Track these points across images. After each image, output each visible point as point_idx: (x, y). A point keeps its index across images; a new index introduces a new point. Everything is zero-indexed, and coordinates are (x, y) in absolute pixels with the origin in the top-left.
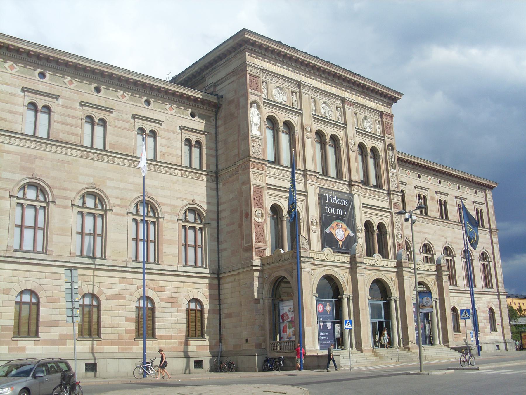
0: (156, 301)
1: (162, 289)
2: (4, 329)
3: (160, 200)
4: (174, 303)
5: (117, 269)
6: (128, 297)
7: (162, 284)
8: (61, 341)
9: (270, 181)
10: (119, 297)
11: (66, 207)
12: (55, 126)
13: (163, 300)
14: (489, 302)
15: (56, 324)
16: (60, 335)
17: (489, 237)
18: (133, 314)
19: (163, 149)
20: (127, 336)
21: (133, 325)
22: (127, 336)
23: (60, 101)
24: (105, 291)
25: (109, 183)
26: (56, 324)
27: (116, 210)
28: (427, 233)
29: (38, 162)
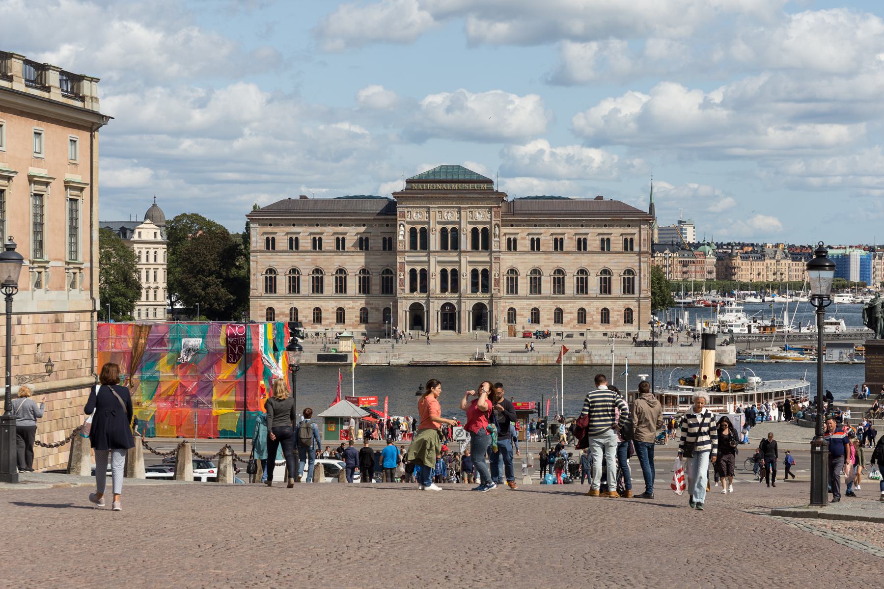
0: (369, 309)
1: (372, 304)
2: (309, 321)
3: (371, 267)
4: (377, 310)
5: (351, 298)
6: (356, 308)
7: (371, 302)
8: (330, 324)
9: (407, 259)
10: (353, 308)
11: (329, 276)
12: (323, 245)
13: (371, 308)
14: (626, 304)
15: (328, 319)
16: (330, 323)
17: (638, 257)
18: (359, 315)
19: (372, 245)
20: (356, 323)
21: (359, 319)
22: (356, 323)
23: (325, 234)
24: (347, 306)
25: (347, 264)
26: (328, 319)
27: (350, 274)
28: (561, 262)
29: (318, 260)
